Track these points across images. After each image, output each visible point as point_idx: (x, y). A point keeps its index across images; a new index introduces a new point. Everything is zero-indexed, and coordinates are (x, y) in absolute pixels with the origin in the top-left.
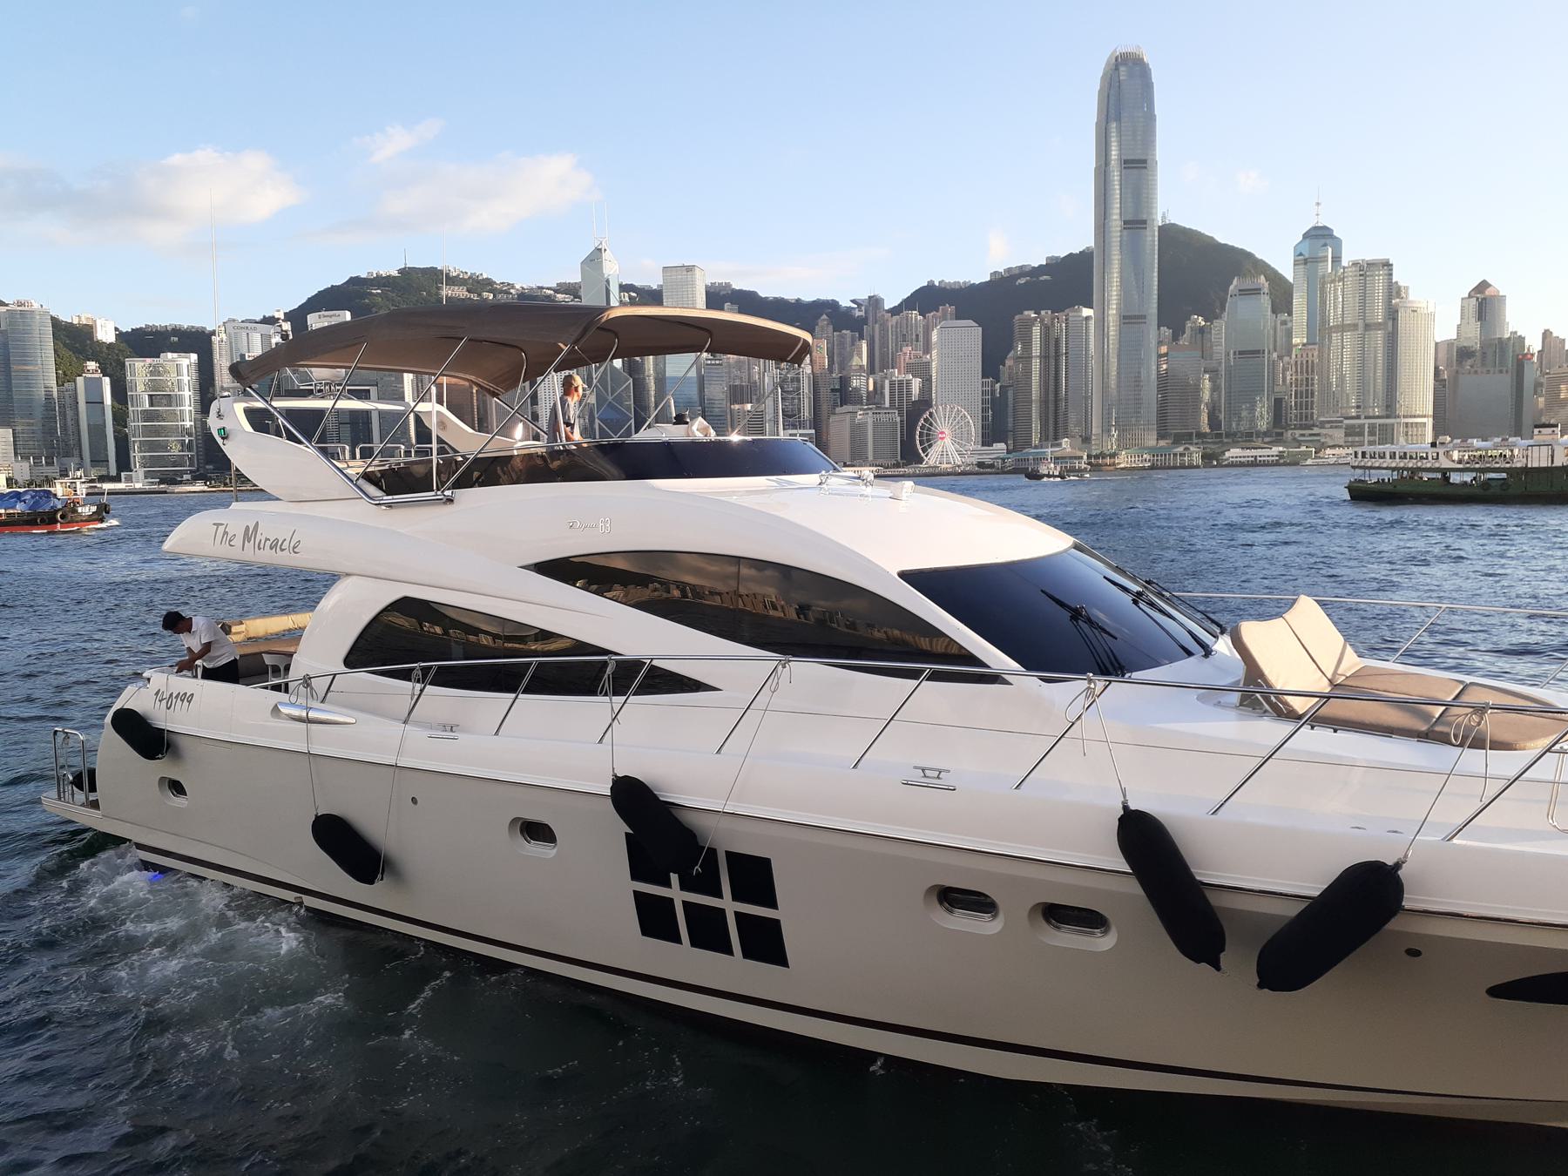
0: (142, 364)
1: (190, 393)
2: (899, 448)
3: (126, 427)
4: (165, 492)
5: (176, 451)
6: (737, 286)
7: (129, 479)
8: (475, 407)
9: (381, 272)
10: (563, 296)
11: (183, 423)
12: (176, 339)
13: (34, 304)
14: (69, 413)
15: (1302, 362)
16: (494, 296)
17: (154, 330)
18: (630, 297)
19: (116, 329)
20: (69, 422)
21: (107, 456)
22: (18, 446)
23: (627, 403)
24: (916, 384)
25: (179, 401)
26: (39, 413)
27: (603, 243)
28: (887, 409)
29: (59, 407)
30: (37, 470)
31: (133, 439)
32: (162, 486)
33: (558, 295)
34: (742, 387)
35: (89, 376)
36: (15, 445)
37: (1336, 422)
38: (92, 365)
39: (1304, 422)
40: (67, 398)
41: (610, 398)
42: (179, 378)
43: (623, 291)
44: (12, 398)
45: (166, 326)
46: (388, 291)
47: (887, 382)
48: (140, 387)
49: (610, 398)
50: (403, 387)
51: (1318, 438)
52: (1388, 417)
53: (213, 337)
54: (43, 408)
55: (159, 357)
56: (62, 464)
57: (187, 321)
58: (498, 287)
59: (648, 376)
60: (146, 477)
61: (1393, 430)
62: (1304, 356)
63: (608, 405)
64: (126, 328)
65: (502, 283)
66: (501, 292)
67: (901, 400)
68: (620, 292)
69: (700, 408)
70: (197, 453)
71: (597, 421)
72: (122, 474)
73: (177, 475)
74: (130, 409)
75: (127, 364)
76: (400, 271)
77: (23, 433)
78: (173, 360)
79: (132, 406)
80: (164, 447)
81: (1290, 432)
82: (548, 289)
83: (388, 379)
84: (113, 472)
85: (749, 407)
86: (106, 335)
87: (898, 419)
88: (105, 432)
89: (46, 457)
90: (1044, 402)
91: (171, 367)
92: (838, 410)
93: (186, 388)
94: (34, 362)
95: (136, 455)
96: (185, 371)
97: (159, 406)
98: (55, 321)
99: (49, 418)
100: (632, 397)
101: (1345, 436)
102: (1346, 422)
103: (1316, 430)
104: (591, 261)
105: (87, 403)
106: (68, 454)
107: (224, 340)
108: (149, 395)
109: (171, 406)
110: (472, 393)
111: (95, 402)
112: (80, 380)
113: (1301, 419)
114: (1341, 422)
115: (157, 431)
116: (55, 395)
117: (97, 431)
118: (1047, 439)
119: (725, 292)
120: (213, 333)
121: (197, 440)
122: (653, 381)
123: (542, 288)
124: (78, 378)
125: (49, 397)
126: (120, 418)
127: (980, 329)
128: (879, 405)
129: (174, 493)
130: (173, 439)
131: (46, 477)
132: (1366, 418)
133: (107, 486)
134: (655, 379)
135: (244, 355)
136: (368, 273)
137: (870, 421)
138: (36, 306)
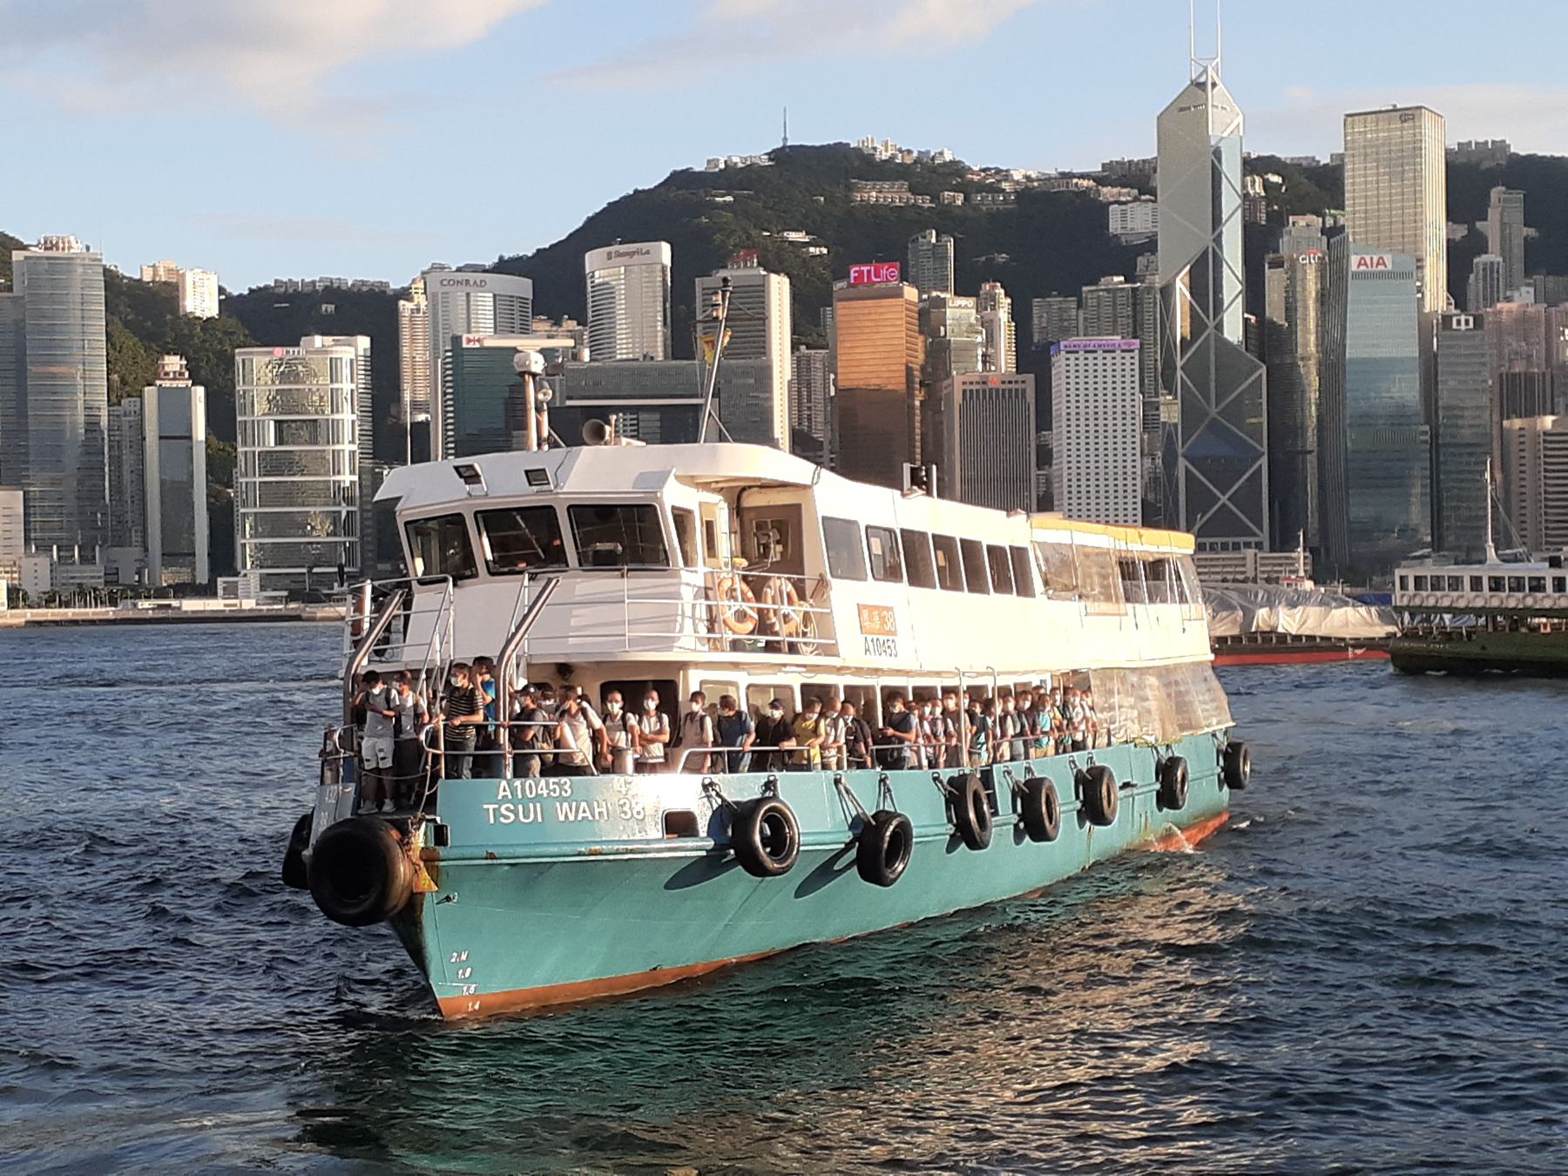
0: (267, 359)
1: (354, 417)
3: (232, 487)
4: (298, 618)
5: (321, 534)
6: (1520, 148)
7: (231, 592)
8: (918, 437)
9: (735, 159)
10: (1116, 190)
11: (337, 478)
12: (331, 308)
13: (73, 244)
14: (128, 458)
16: (965, 199)
17: (291, 291)
18: (1267, 185)
19: (221, 290)
20: (127, 477)
21: (192, 543)
22: (32, 526)
23: (1253, 420)
25: (332, 432)
26: (72, 457)
27: (1210, 69)
29: (110, 448)
30: (64, 573)
31: (242, 510)
32: (292, 605)
33: (1105, 190)
34: (1529, 378)
35: (166, 384)
36: (26, 523)
38: (173, 363)
40: (126, 427)
41: (1213, 411)
42: (335, 386)
43: (1251, 173)
44: (27, 431)
45: (313, 283)
46: (749, 197)
48: (260, 407)
49: (1213, 411)
50: (770, 399)
53: (402, 302)
54: (80, 450)
55: (298, 345)
56: (109, 560)
57: (352, 271)
58: (976, 178)
59: (1302, 359)
60: (263, 588)
63: (1209, 427)
64: (238, 288)
65: (984, 170)
66: (981, 187)
68: (1244, 175)
69: (1427, 428)
70: (362, 538)
71: (1182, 463)
72: (220, 580)
73: (321, 583)
74: (240, 449)
75: (239, 359)
76: (775, 155)
77: (41, 499)
78: (323, 351)
79: (245, 443)
80: (297, 524)
82: (1082, 176)
83: (741, 381)
84: (202, 577)
85: (1548, 421)
86: (201, 302)
88: (190, 495)
89: (79, 547)
91: (320, 365)
93: (347, 407)
94: (67, 359)
95: (247, 542)
96: (346, 371)
97: (294, 443)
98: (112, 280)
99: (91, 470)
100: (1265, 406)
104: (1181, 110)
105: (161, 438)
106: (121, 541)
107: (423, 307)
108: (276, 421)
109: (316, 443)
110: (912, 407)
111: (177, 436)
112: (150, 392)
115: (289, 494)
116: (104, 422)
117: (176, 494)
119: (1493, 164)
120: (405, 294)
121: (362, 511)
122: (1314, 371)
123: (1070, 176)
124: (146, 389)
125: (92, 426)
126: (221, 467)
129: (314, 619)
130: (318, 509)
131: (80, 585)
133: (191, 605)
134: (1320, 364)
135: (461, 337)
136: (709, 162)
138: (77, 248)
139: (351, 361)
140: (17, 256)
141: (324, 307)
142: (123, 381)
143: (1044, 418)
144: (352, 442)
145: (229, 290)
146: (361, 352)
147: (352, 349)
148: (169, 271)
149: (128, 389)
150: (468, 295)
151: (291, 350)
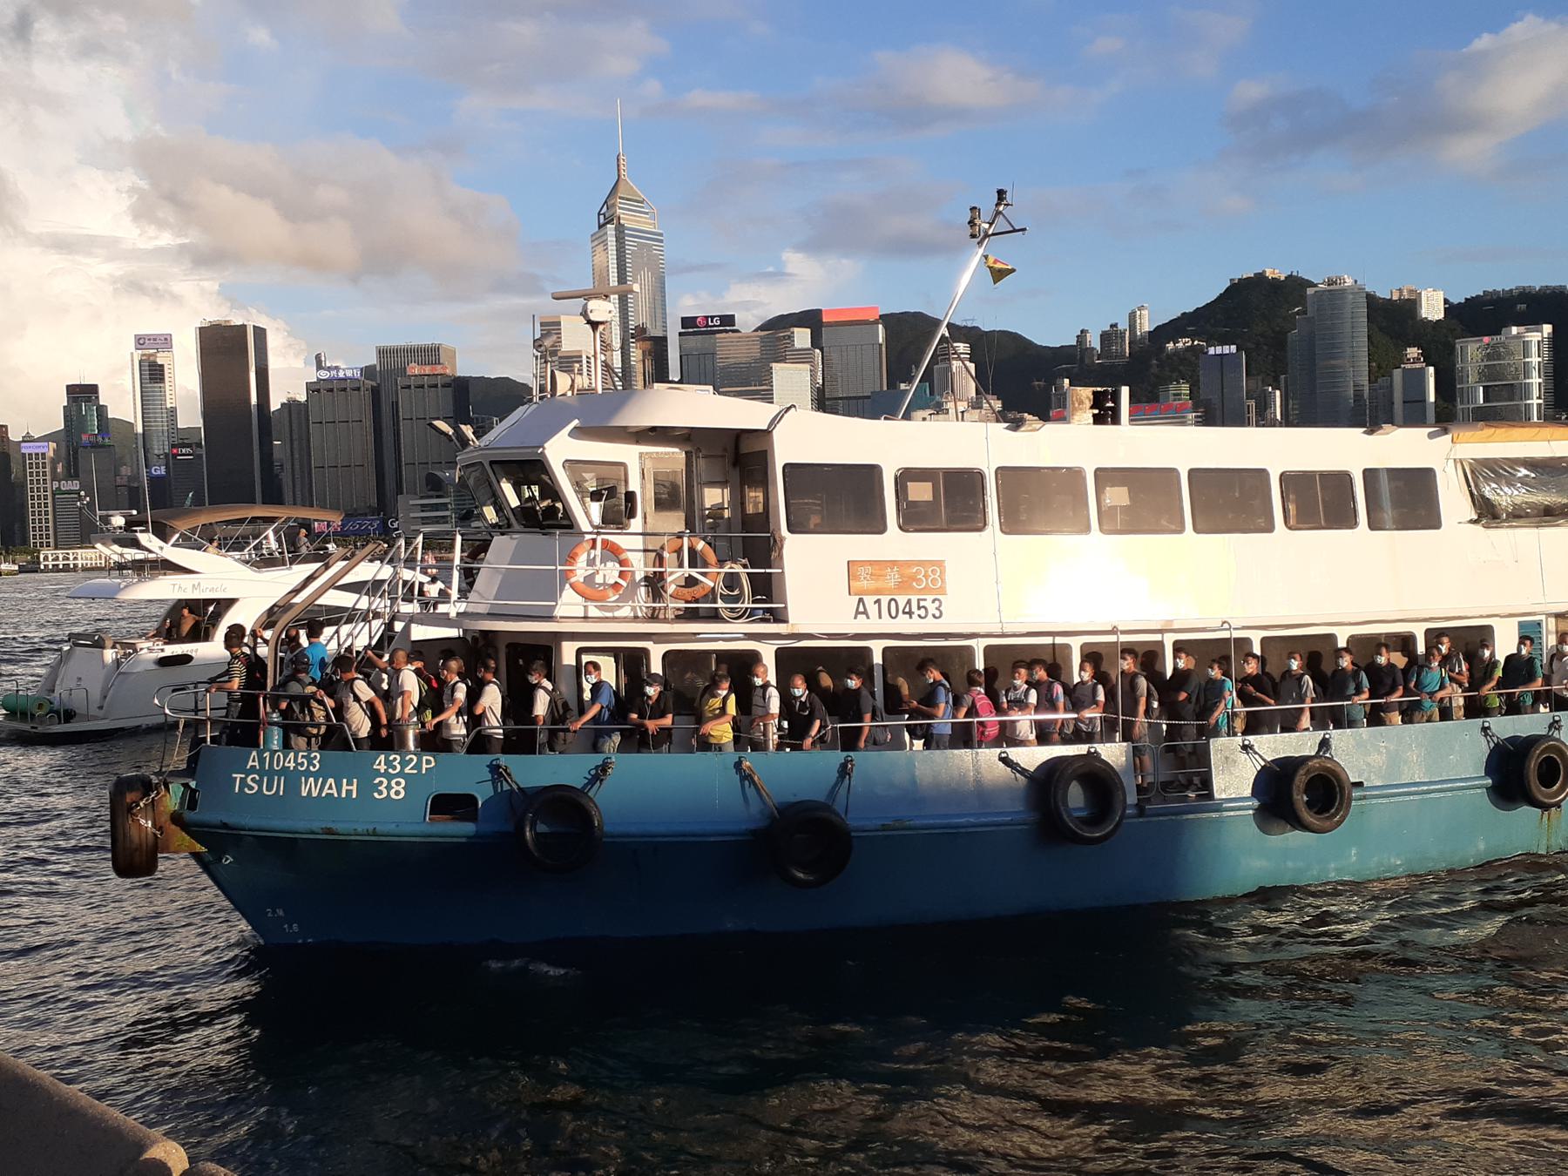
0: (1478, 346)
1: (1541, 380)
12: (1524, 306)
17: (1495, 297)
19: (1446, 301)
35: (1408, 366)
38: (1413, 352)
42: (1527, 360)
45: (1511, 290)
48: (1472, 378)
75: (1458, 346)
78: (1519, 336)
79: (1462, 403)
86: (1432, 309)
91: (1516, 347)
93: (1535, 373)
96: (1534, 349)
98: (1371, 299)
105: (1404, 402)
138: (1349, 282)
139: (1539, 342)
140: (1310, 291)
141: (1519, 306)
142: (1379, 367)
144: (1539, 398)
145: (1451, 300)
146: (1546, 335)
147: (1540, 334)
148: (1411, 291)
149: (1382, 371)
151: (1495, 338)
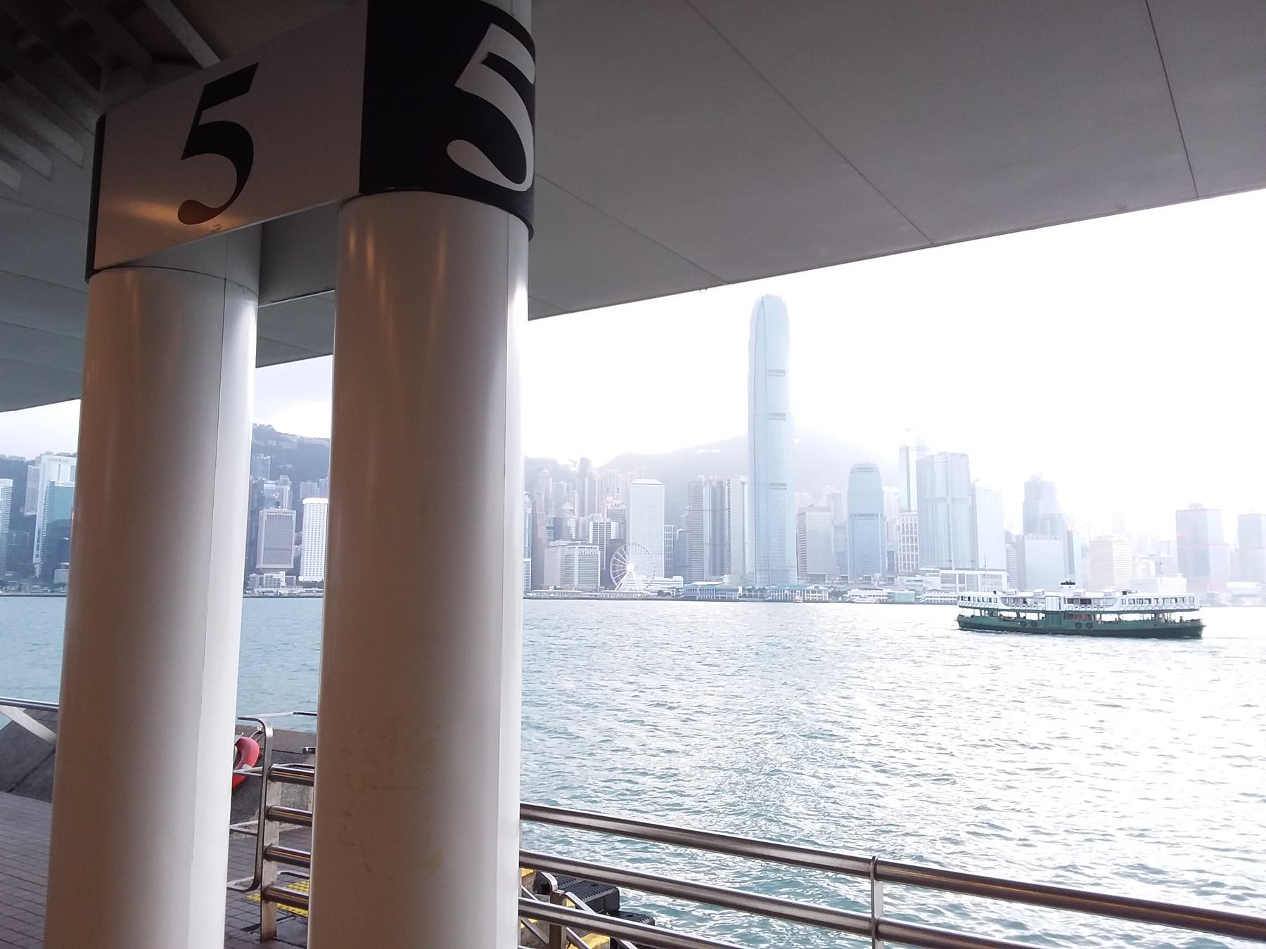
2: (599, 577)
15: (907, 524)
24: (614, 524)
28: (589, 544)
37: (934, 571)
39: (911, 571)
47: (591, 523)
51: (921, 583)
52: (973, 569)
61: (977, 579)
62: (905, 520)
67: (602, 539)
81: (899, 578)
87: (599, 553)
90: (713, 544)
92: (552, 543)
101: (942, 583)
102: (941, 572)
103: (918, 577)
113: (909, 569)
114: (938, 572)
118: (715, 575)
127: (663, 486)
128: (584, 541)
132: (956, 569)
137: (576, 552)
143: (299, 527)
150: (60, 465)
